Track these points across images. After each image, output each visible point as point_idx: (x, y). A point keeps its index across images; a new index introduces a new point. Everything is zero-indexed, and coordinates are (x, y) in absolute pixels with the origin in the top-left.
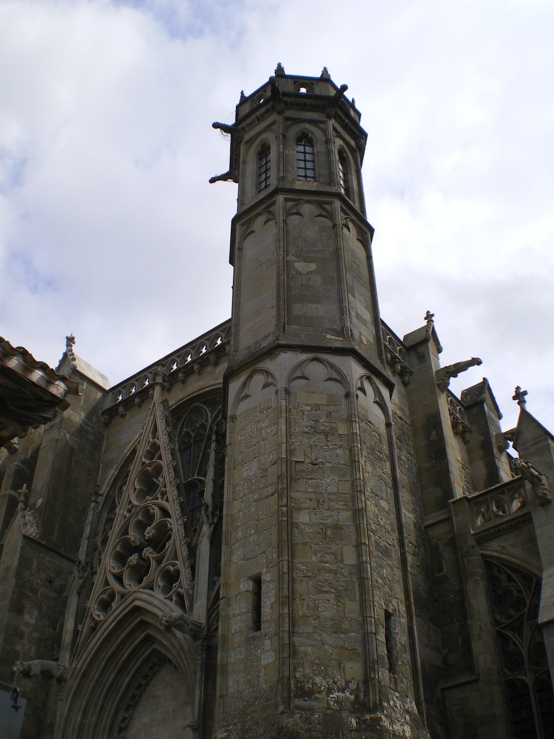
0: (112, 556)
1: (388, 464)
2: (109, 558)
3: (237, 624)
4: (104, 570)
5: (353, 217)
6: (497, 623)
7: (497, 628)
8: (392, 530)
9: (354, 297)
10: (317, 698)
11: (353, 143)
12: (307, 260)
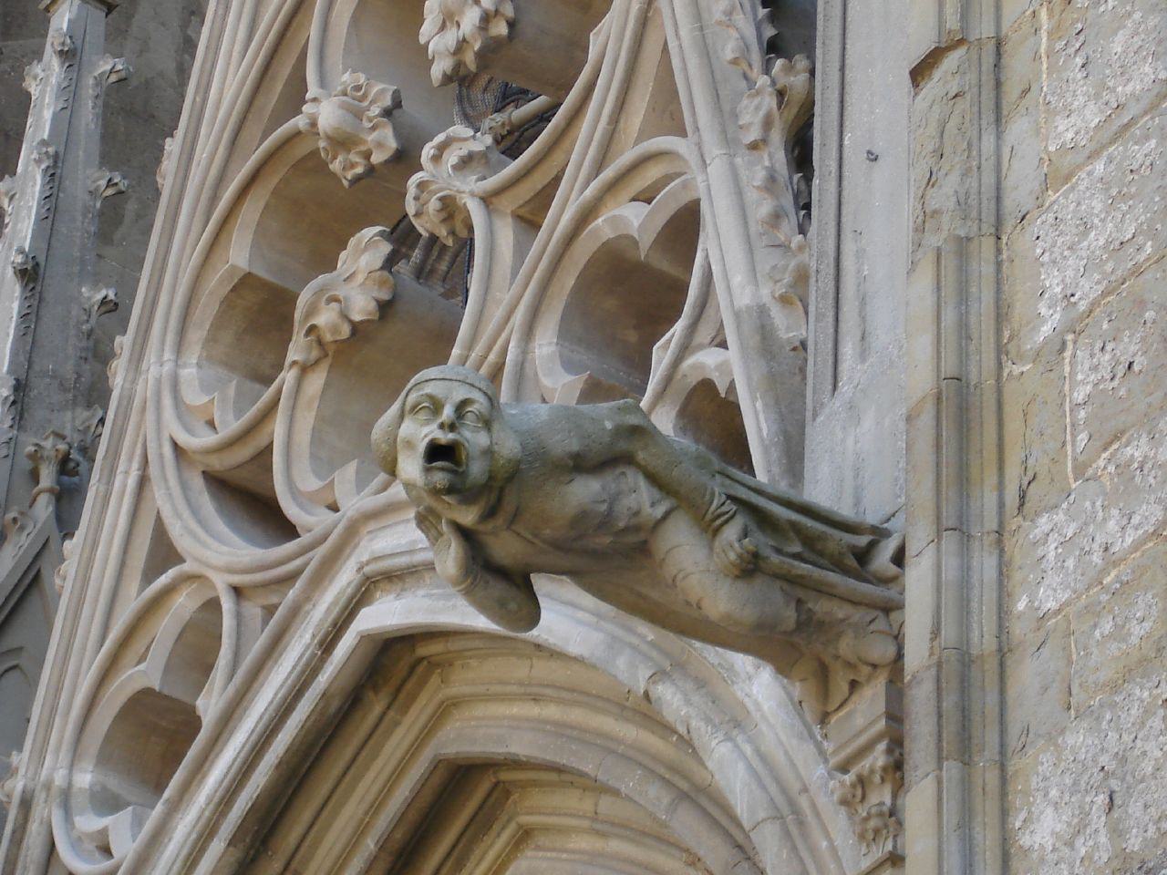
0: (197, 336)
2: (168, 355)
3: (1086, 228)
4: (135, 465)
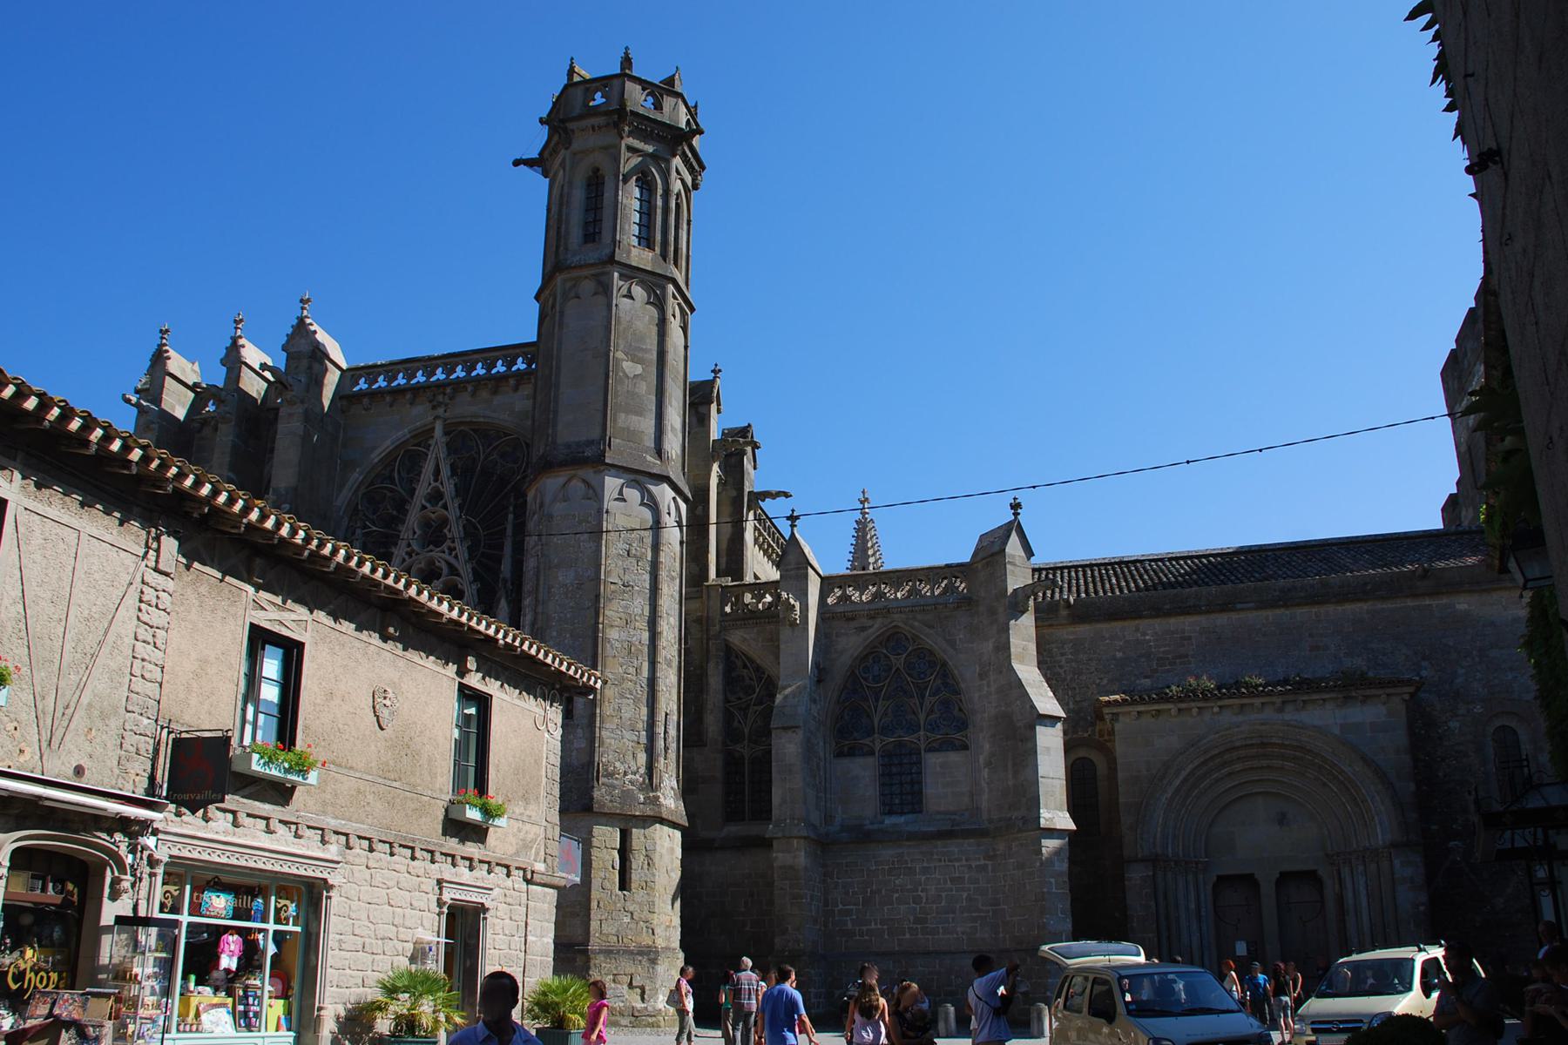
5: (681, 301)
6: (727, 701)
7: (727, 705)
8: (675, 643)
10: (617, 779)
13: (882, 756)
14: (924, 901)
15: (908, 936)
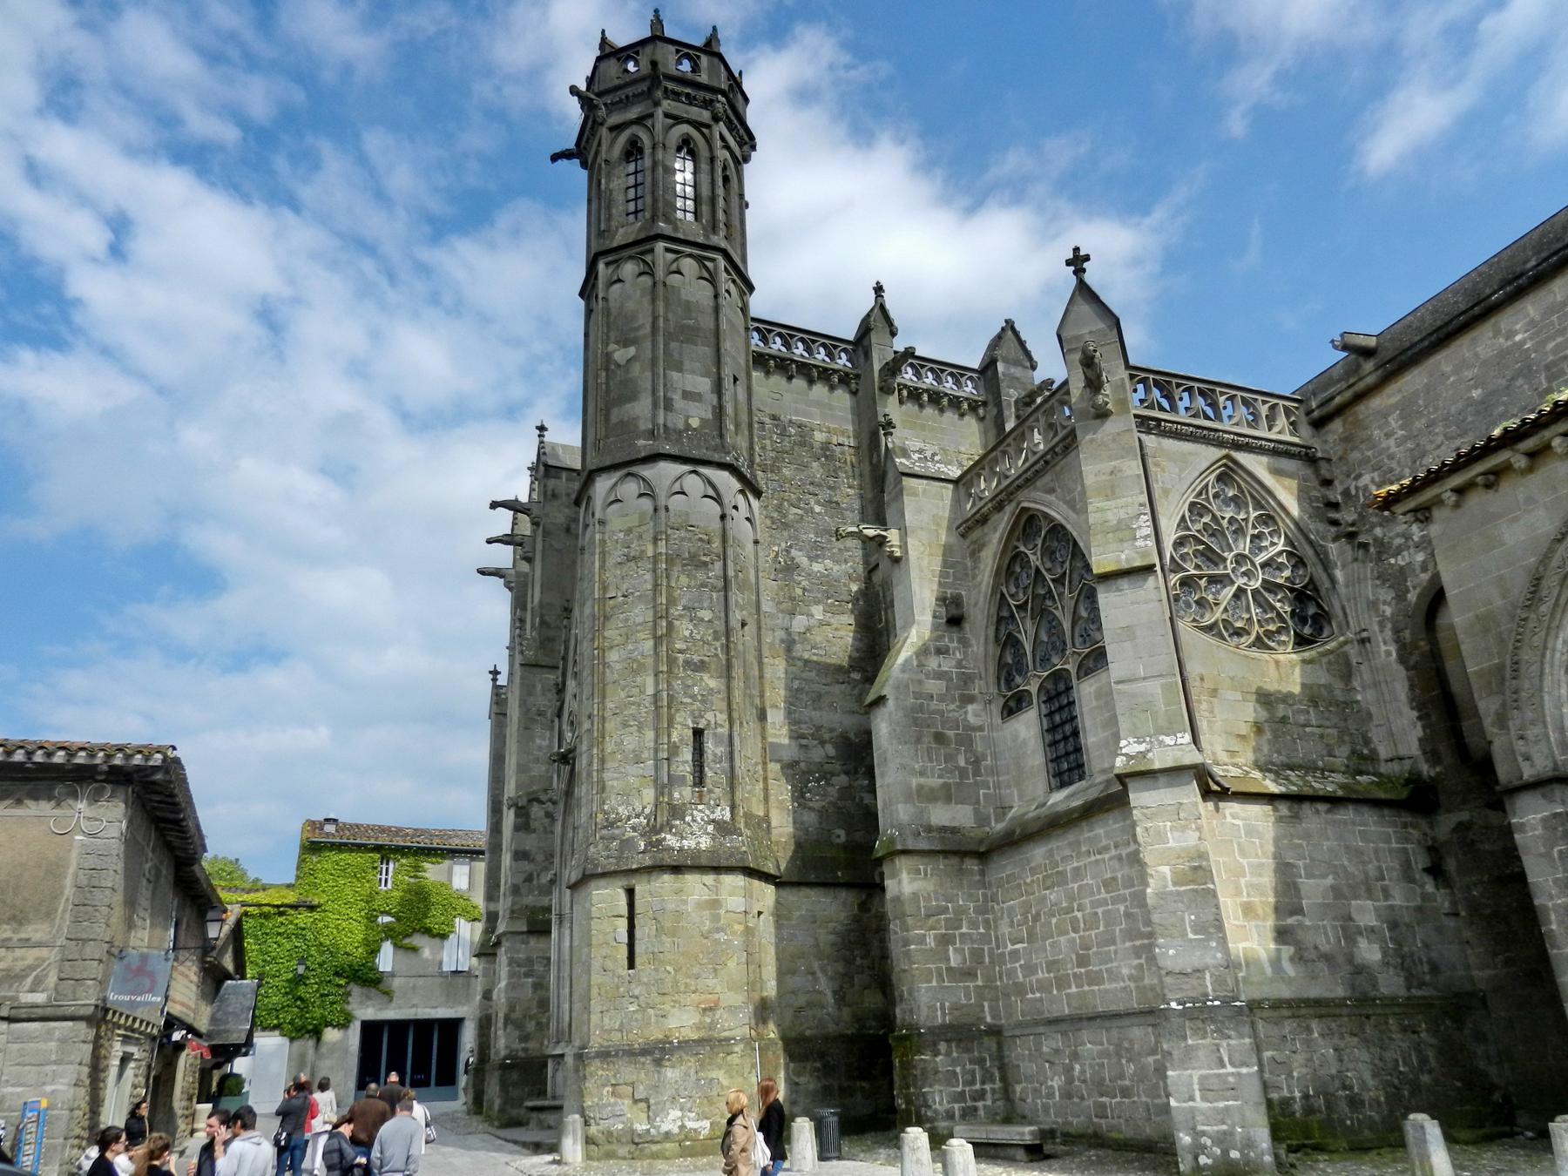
1: (718, 565)
5: (688, 250)
8: (716, 639)
9: (680, 370)
11: (705, 116)
12: (626, 343)
13: (1044, 702)
14: (1082, 925)
15: (1074, 989)
